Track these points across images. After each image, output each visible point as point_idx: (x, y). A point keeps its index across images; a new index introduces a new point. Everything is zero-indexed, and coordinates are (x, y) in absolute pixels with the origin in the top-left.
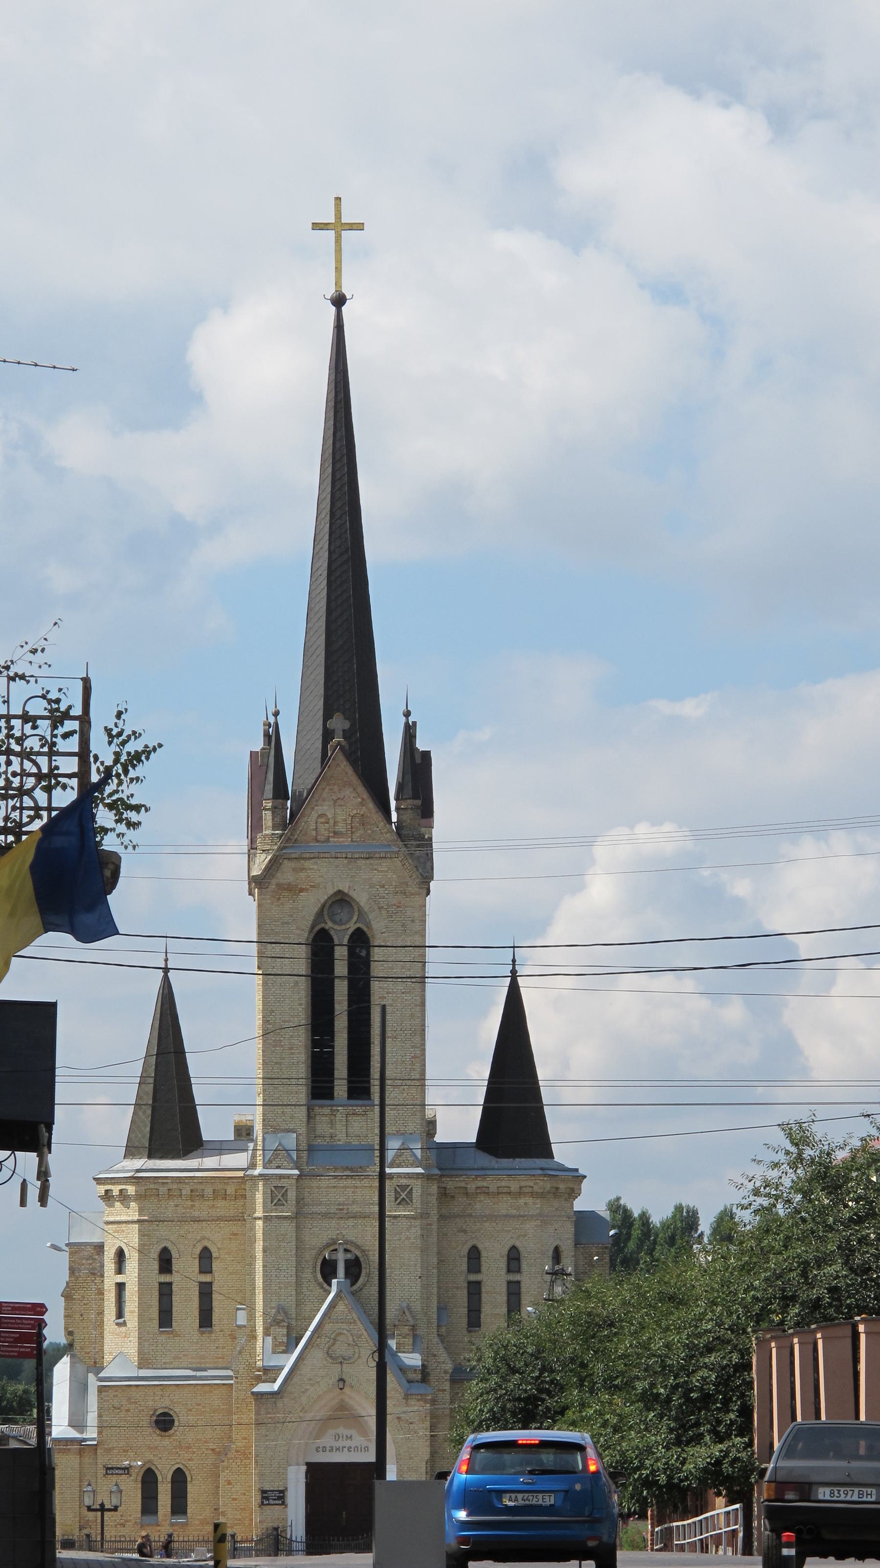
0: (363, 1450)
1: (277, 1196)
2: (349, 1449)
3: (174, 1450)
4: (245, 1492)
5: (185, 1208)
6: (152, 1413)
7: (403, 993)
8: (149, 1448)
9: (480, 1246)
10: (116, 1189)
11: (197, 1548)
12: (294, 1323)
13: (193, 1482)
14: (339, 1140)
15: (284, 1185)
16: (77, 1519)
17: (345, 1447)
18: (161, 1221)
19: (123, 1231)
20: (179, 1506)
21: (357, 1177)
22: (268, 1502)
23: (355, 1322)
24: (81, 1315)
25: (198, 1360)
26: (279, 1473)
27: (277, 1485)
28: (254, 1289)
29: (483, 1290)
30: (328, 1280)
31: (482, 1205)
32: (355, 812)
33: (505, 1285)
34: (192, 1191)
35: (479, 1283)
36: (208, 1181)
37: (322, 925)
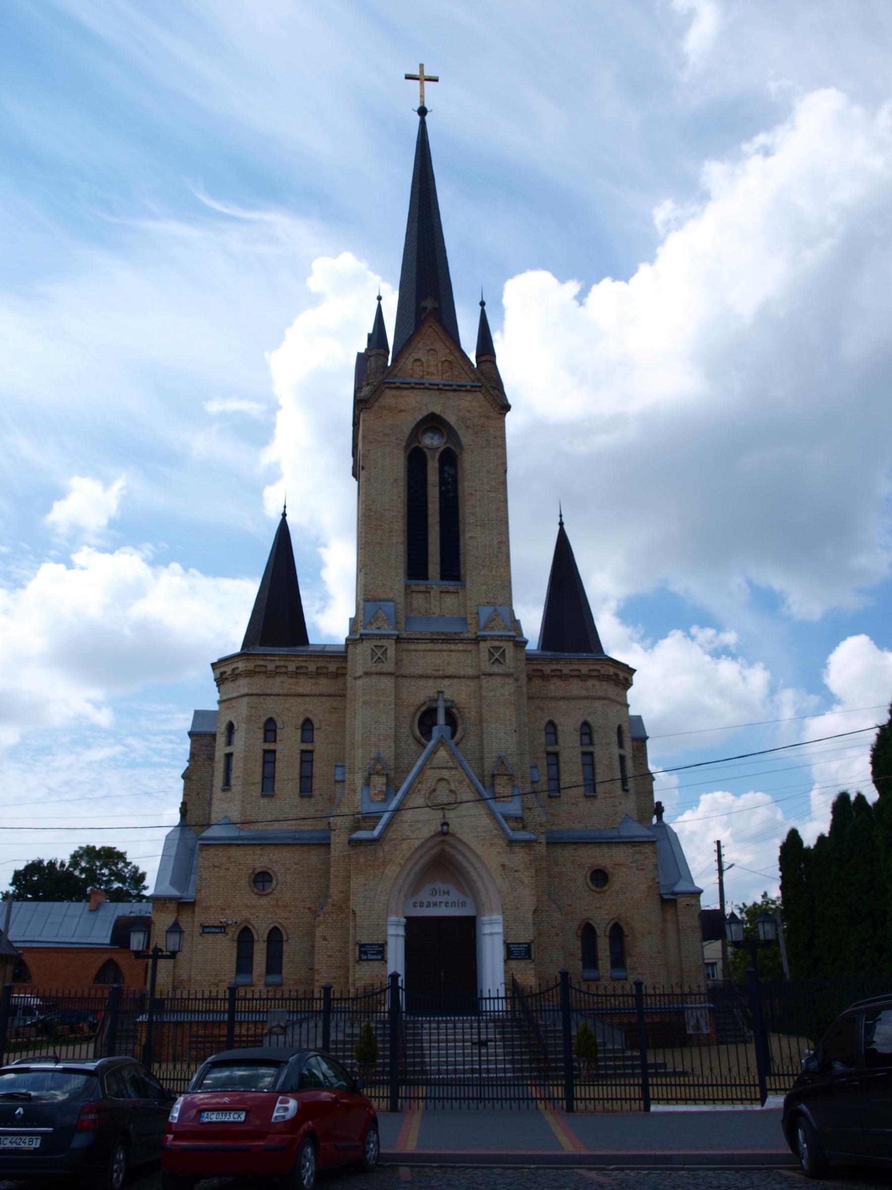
0: (460, 906)
1: (377, 654)
2: (446, 904)
4: (341, 948)
5: (290, 684)
6: (250, 872)
7: (489, 491)
8: (247, 906)
9: (556, 721)
10: (228, 669)
11: (271, 1010)
12: (392, 774)
13: (290, 941)
14: (434, 614)
15: (383, 645)
16: (171, 978)
17: (442, 902)
18: (267, 695)
19: (234, 707)
20: (274, 964)
21: (452, 641)
22: (366, 957)
23: (456, 768)
24: (198, 794)
26: (378, 925)
27: (376, 939)
28: (353, 744)
29: (561, 760)
30: (427, 733)
31: (555, 687)
32: (444, 359)
33: (580, 755)
34: (297, 668)
35: (556, 754)
36: (312, 659)
37: (417, 444)
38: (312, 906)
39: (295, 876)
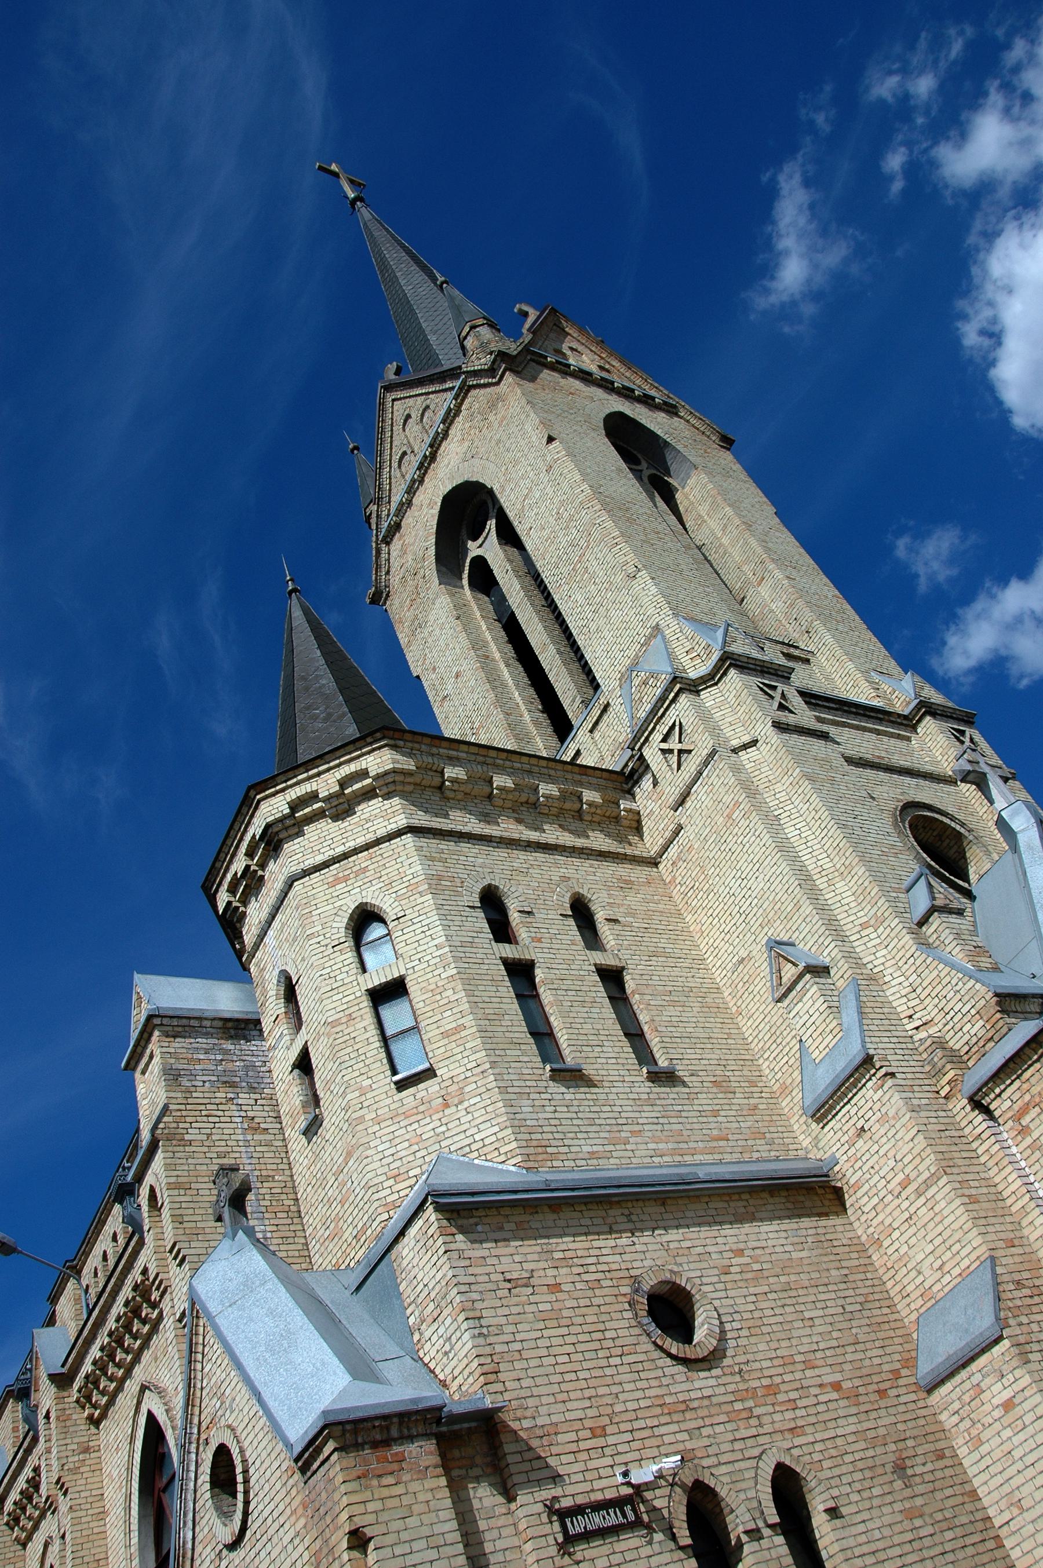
3: (738, 1406)
19: (365, 870)
25: (670, 1146)
38: (838, 1377)
39: (752, 1290)
